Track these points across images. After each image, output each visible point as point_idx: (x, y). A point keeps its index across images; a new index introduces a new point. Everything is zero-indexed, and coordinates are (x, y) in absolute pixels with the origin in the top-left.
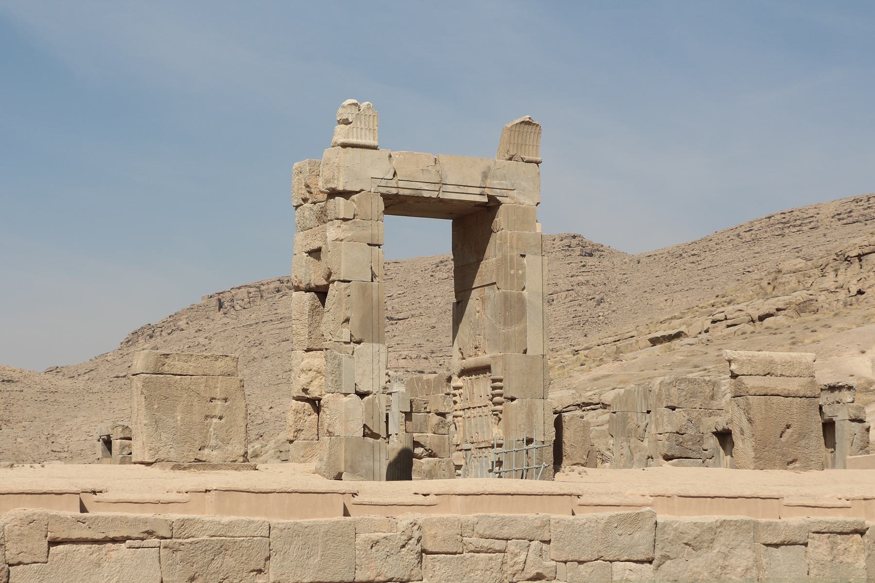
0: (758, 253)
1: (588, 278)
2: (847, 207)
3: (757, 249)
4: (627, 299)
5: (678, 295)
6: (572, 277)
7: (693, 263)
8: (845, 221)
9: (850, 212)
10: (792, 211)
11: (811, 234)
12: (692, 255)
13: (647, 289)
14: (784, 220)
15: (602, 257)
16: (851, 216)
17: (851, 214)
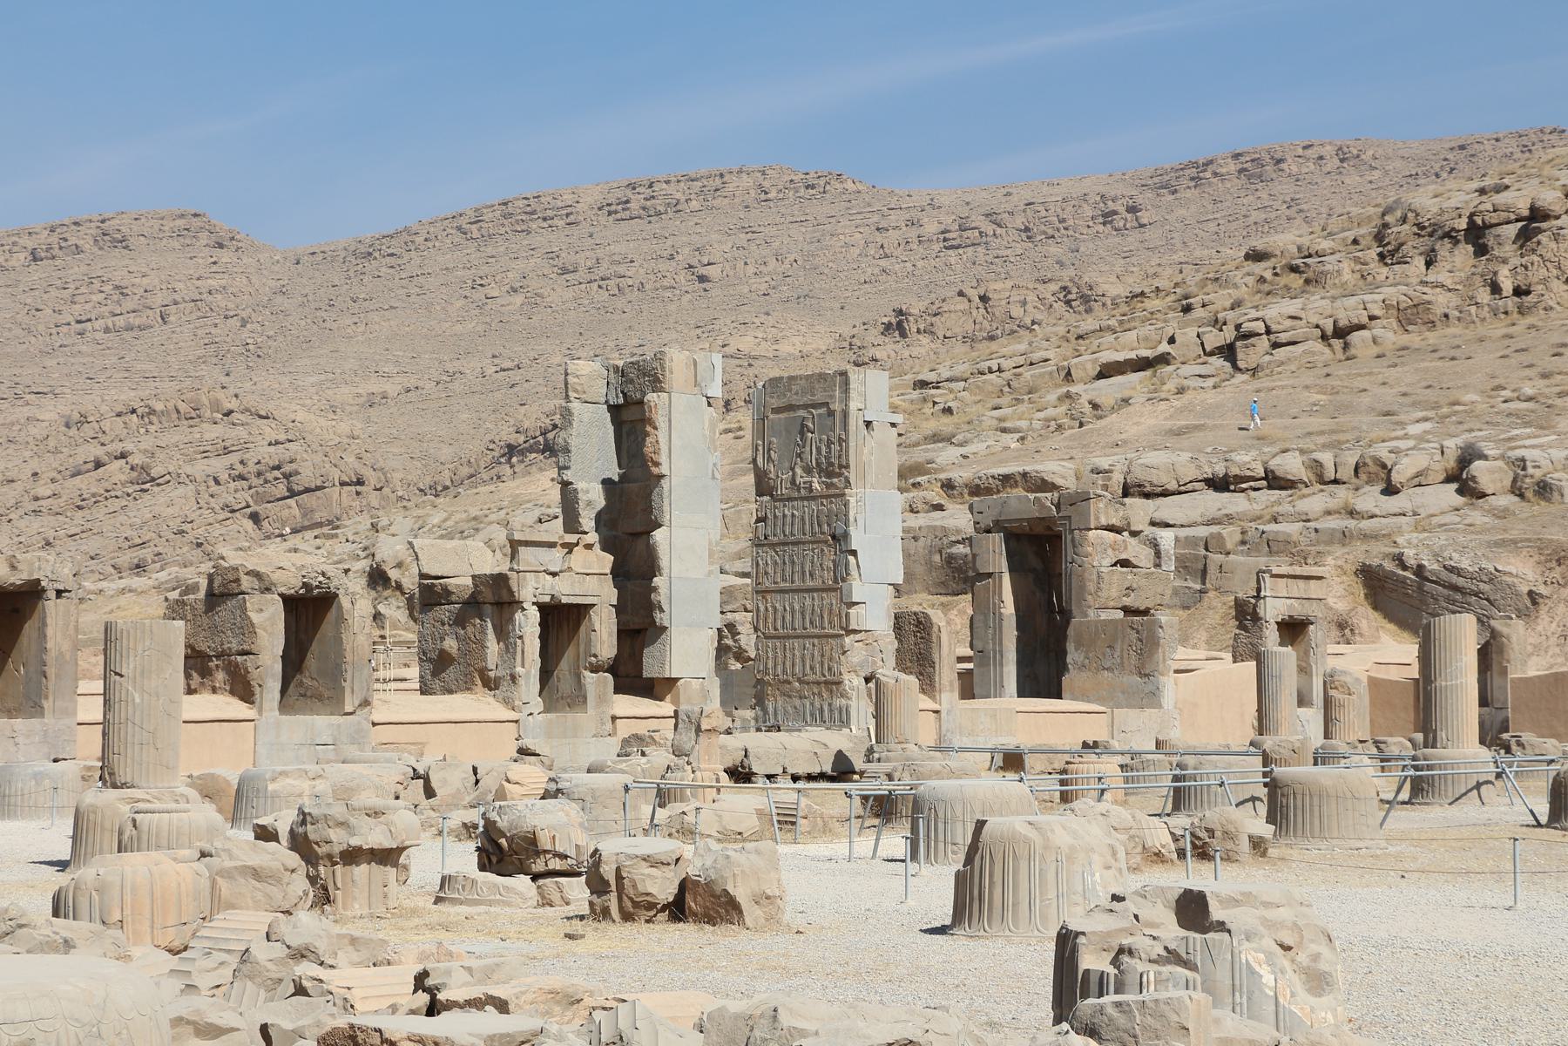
0: (493, 257)
1: (223, 282)
2: (619, 194)
3: (490, 250)
4: (291, 319)
5: (375, 317)
6: (198, 279)
7: (392, 267)
8: (618, 216)
9: (627, 202)
10: (539, 196)
11: (569, 233)
12: (388, 255)
13: (322, 305)
14: (529, 209)
15: (240, 251)
16: (628, 209)
17: (628, 205)
